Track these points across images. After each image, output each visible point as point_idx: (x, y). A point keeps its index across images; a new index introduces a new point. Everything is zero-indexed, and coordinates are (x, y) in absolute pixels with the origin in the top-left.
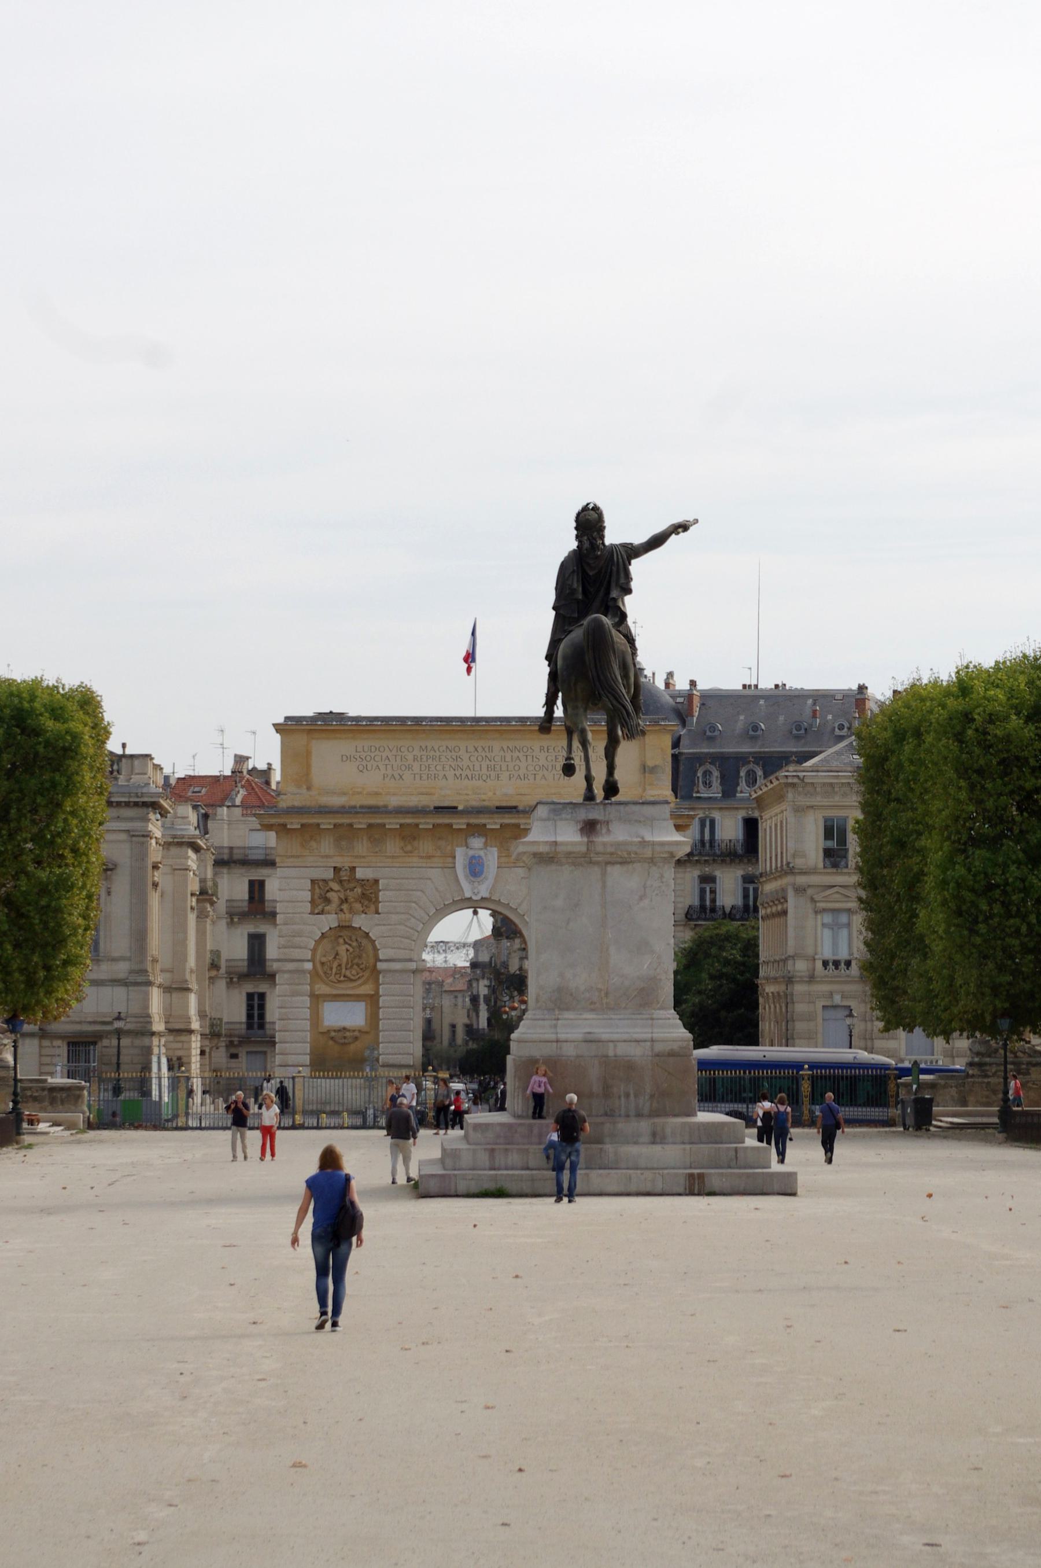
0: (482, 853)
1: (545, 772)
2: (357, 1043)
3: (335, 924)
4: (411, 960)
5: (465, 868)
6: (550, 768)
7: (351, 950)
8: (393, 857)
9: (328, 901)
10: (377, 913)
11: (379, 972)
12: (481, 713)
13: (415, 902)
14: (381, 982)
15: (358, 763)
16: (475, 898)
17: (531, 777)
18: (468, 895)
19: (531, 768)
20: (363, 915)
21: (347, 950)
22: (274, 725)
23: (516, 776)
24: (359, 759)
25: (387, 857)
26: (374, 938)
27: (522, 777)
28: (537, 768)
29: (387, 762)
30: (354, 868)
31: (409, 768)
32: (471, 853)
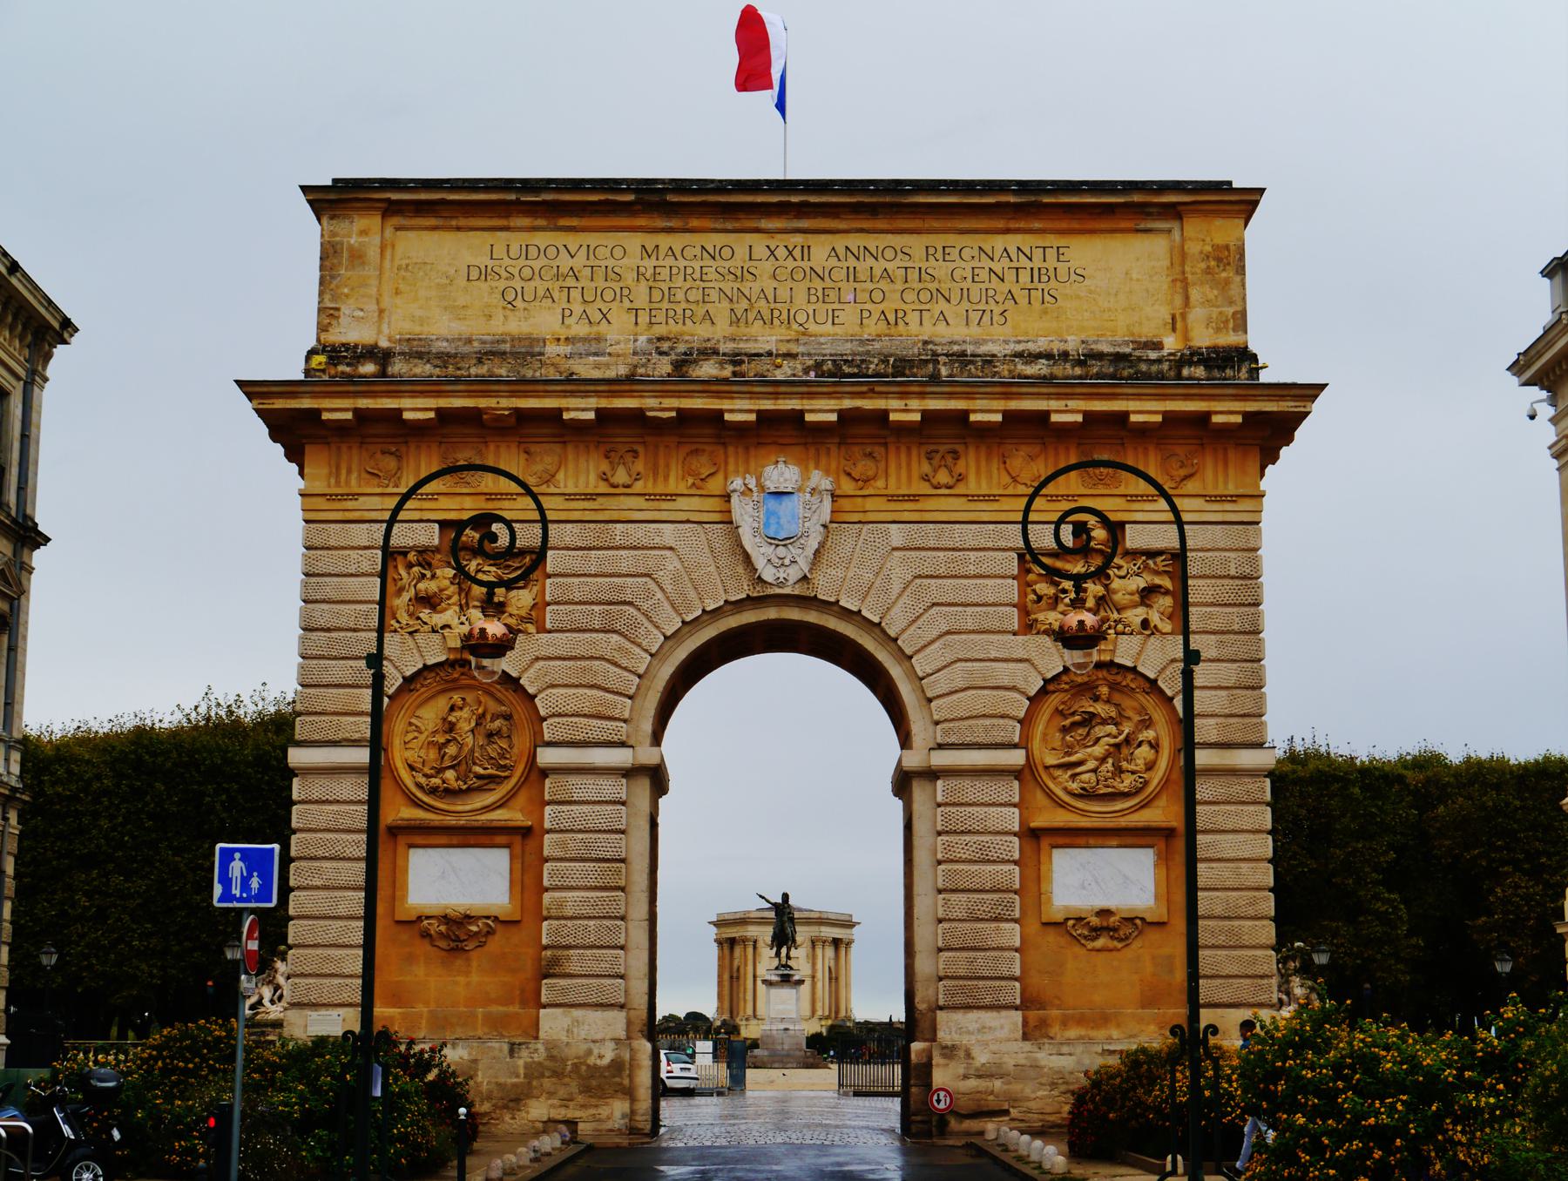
1: (942, 303)
4: (623, 744)
6: (955, 298)
11: (545, 773)
12: (791, 176)
13: (630, 604)
15: (502, 284)
17: (913, 318)
19: (910, 297)
22: (305, 189)
23: (876, 315)
24: (504, 275)
27: (891, 318)
28: (925, 296)
29: (571, 282)
31: (624, 294)
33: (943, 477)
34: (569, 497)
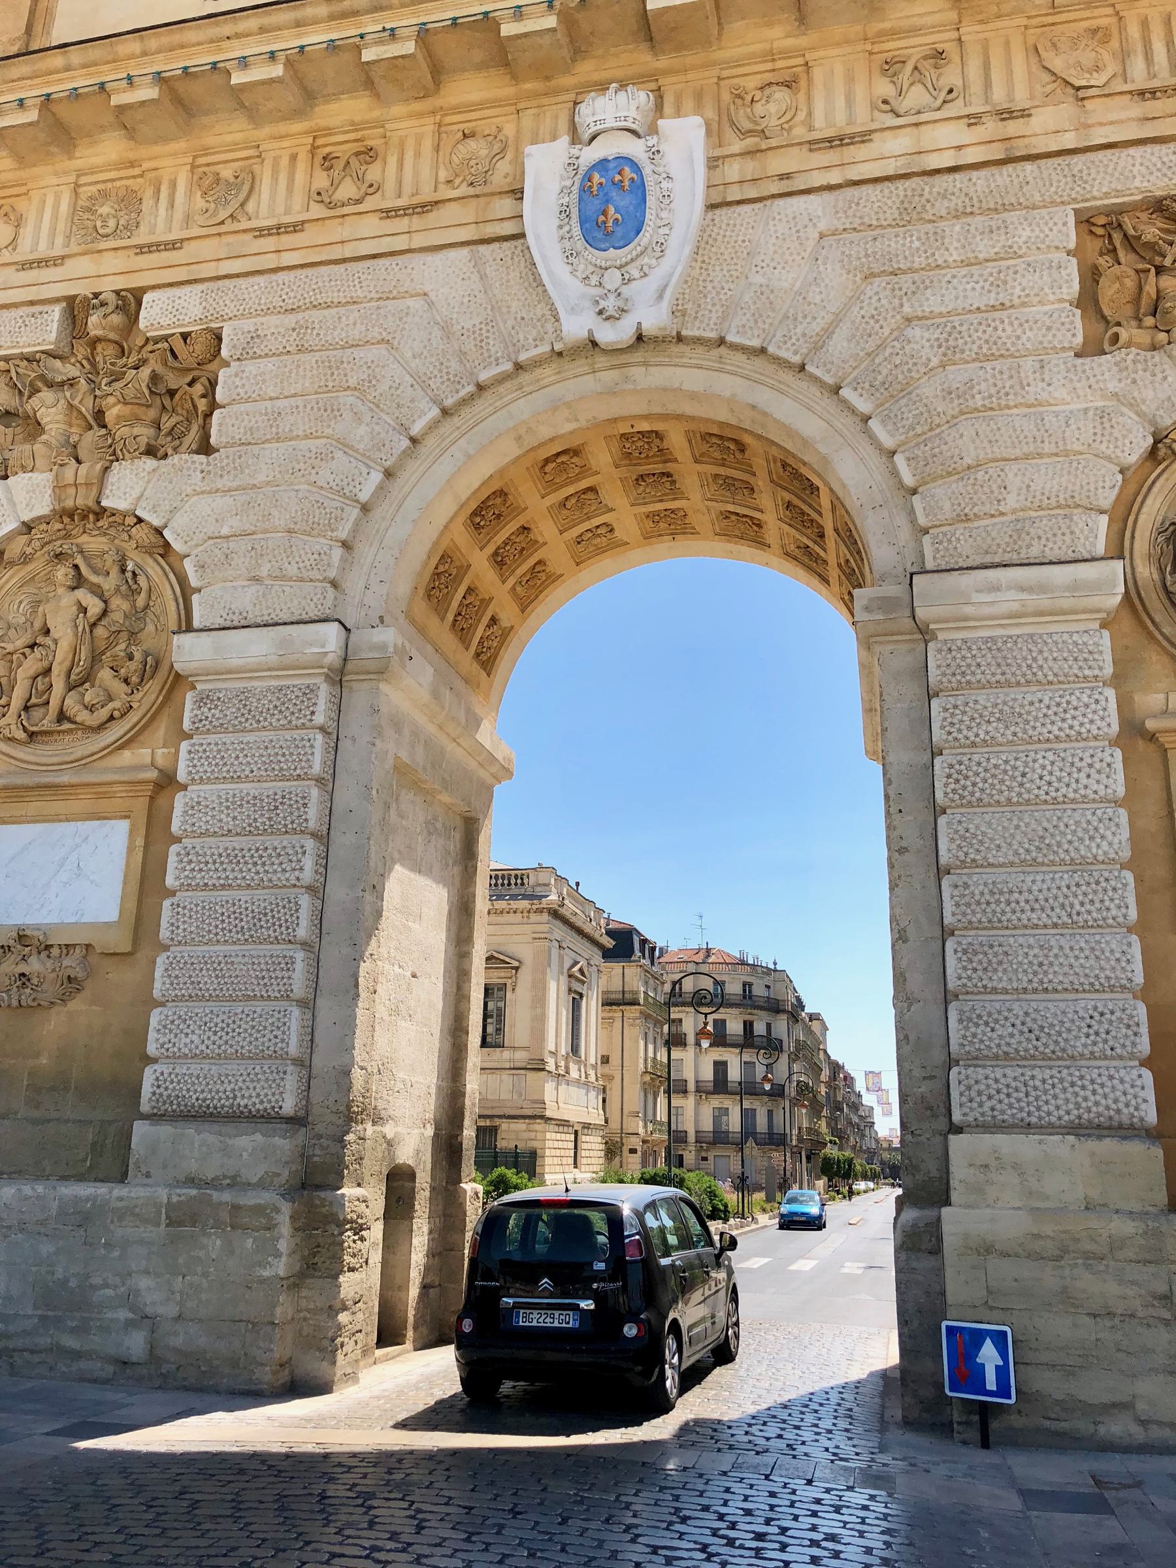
0: (635, 148)
2: (73, 1005)
3: (43, 507)
5: (565, 212)
7: (95, 606)
8: (278, 230)
9: (34, 428)
10: (205, 448)
14: (187, 725)
16: (607, 335)
18: (576, 327)
20: (150, 463)
21: (85, 611)
25: (262, 232)
26: (177, 546)
30: (138, 295)
32: (590, 155)
33: (916, 96)
34: (262, 232)
